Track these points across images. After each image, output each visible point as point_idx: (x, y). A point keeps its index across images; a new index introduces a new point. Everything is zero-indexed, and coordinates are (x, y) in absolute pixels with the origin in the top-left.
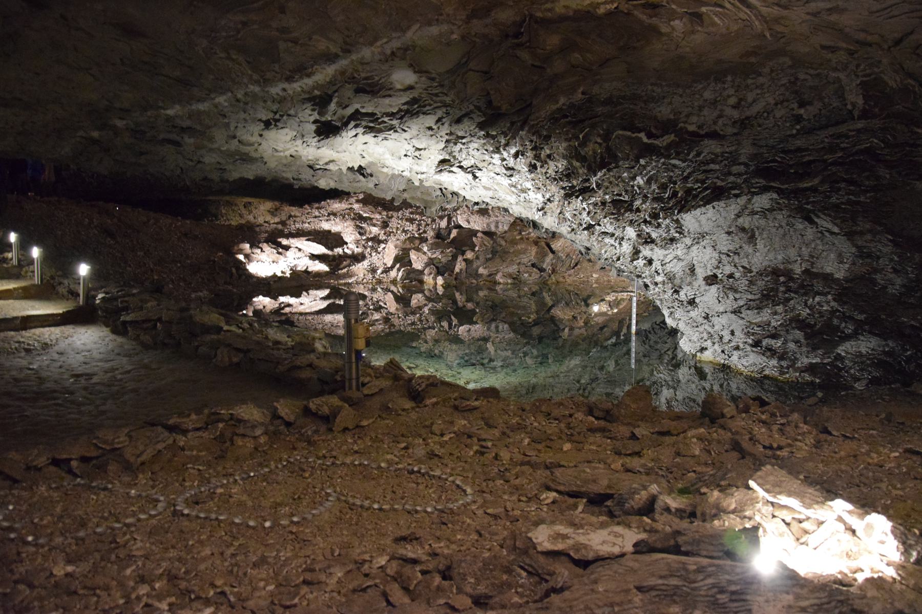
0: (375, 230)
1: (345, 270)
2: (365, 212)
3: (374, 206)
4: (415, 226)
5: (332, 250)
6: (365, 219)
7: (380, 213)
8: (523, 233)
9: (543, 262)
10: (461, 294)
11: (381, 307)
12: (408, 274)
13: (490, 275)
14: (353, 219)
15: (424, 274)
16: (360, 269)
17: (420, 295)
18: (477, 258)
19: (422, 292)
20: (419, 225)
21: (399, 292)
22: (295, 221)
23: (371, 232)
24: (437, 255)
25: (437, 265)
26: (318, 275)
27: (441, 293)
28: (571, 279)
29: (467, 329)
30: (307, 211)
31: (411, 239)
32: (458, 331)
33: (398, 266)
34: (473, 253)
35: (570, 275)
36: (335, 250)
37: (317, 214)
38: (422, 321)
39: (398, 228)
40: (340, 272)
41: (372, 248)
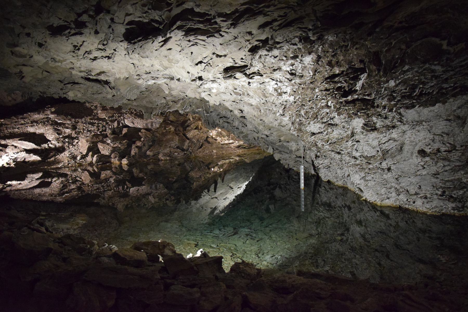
0: (68, 131)
1: (53, 159)
2: (59, 120)
3: (65, 116)
4: (95, 127)
5: (40, 146)
6: (60, 124)
7: (70, 120)
8: (167, 129)
9: (184, 145)
10: (137, 169)
11: (77, 181)
12: (100, 159)
13: (154, 155)
14: (52, 125)
15: (111, 158)
16: (64, 157)
17: (109, 172)
18: (144, 145)
19: (110, 168)
20: (98, 126)
21: (94, 170)
22: (6, 128)
23: (65, 133)
24: (118, 145)
25: (119, 151)
26: (34, 163)
27: (126, 169)
28: (200, 154)
29: (137, 189)
30: (14, 121)
31: (96, 136)
32: (129, 190)
33: (91, 153)
34: (141, 143)
35: (200, 152)
36: (42, 146)
37: (23, 122)
38: (104, 187)
39: (84, 129)
40: (49, 160)
41: (69, 143)
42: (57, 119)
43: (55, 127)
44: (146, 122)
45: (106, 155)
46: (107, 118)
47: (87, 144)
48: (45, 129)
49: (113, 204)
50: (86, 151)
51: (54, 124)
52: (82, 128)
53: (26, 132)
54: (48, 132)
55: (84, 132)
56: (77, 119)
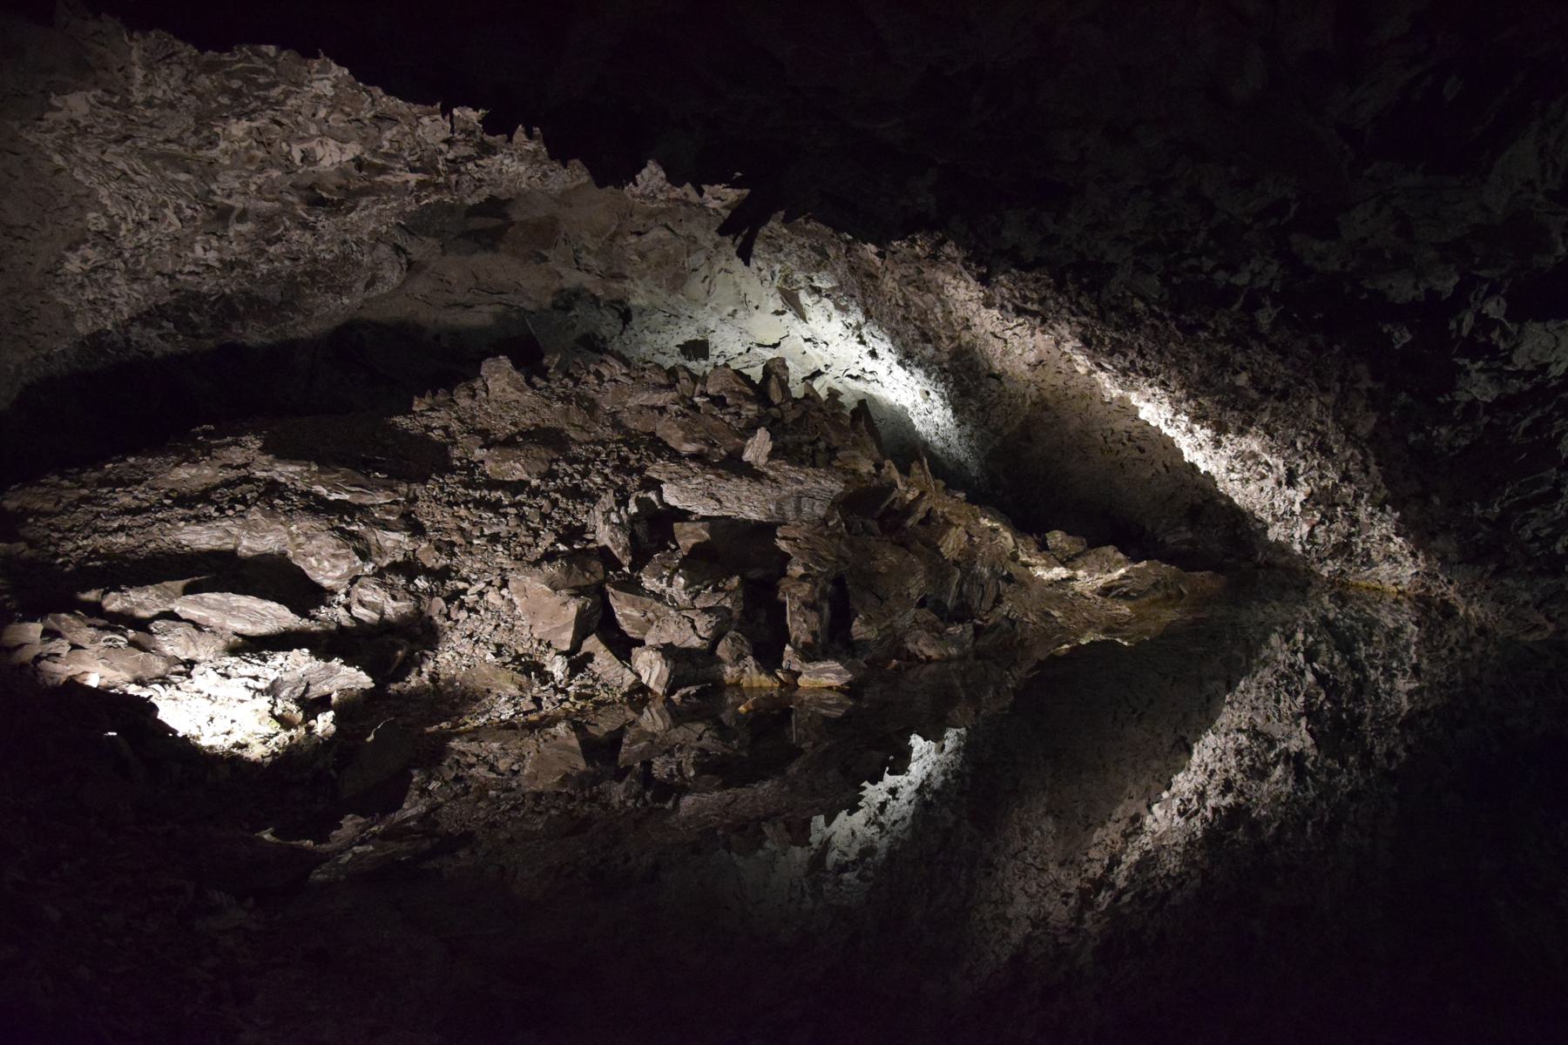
2: (337, 489)
3: (355, 468)
8: (831, 524)
15: (720, 661)
20: (521, 517)
23: (382, 552)
29: (728, 799)
32: (676, 804)
34: (807, 586)
37: (126, 500)
45: (689, 650)
46: (534, 482)
47: (558, 599)
48: (290, 533)
50: (568, 635)
51: (318, 507)
52: (452, 525)
53: (179, 551)
54: (308, 548)
55: (471, 544)
56: (414, 486)
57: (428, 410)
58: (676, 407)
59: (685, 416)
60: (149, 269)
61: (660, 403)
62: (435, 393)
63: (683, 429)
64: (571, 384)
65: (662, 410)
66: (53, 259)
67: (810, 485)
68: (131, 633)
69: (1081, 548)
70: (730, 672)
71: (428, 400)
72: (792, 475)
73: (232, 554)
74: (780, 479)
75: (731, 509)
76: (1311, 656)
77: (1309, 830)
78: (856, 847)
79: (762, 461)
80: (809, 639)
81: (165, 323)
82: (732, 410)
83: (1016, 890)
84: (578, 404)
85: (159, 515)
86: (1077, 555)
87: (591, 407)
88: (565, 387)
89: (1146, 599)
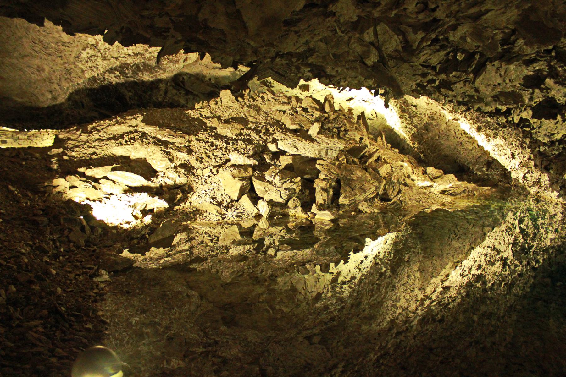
0: (183, 157)
14: (155, 143)
15: (288, 207)
34: (325, 183)
42: (160, 134)
43: (163, 149)
44: (318, 147)
45: (278, 203)
49: (217, 271)
51: (157, 142)
54: (154, 156)
56: (191, 136)
57: (201, 108)
58: (289, 111)
59: (292, 115)
60: (109, 56)
61: (284, 110)
62: (203, 102)
63: (291, 120)
64: (252, 101)
65: (284, 112)
66: (78, 53)
67: (331, 145)
68: (93, 183)
69: (440, 174)
70: (291, 212)
71: (200, 105)
72: (325, 141)
73: (128, 157)
74: (321, 142)
75: (302, 152)
76: (521, 221)
77: (502, 285)
78: (350, 276)
79: (315, 134)
80: (323, 202)
81: (116, 72)
82: (310, 114)
83: (402, 297)
84: (254, 108)
85: (107, 143)
86: (439, 177)
87: (258, 110)
88: (250, 102)
89: (459, 196)
